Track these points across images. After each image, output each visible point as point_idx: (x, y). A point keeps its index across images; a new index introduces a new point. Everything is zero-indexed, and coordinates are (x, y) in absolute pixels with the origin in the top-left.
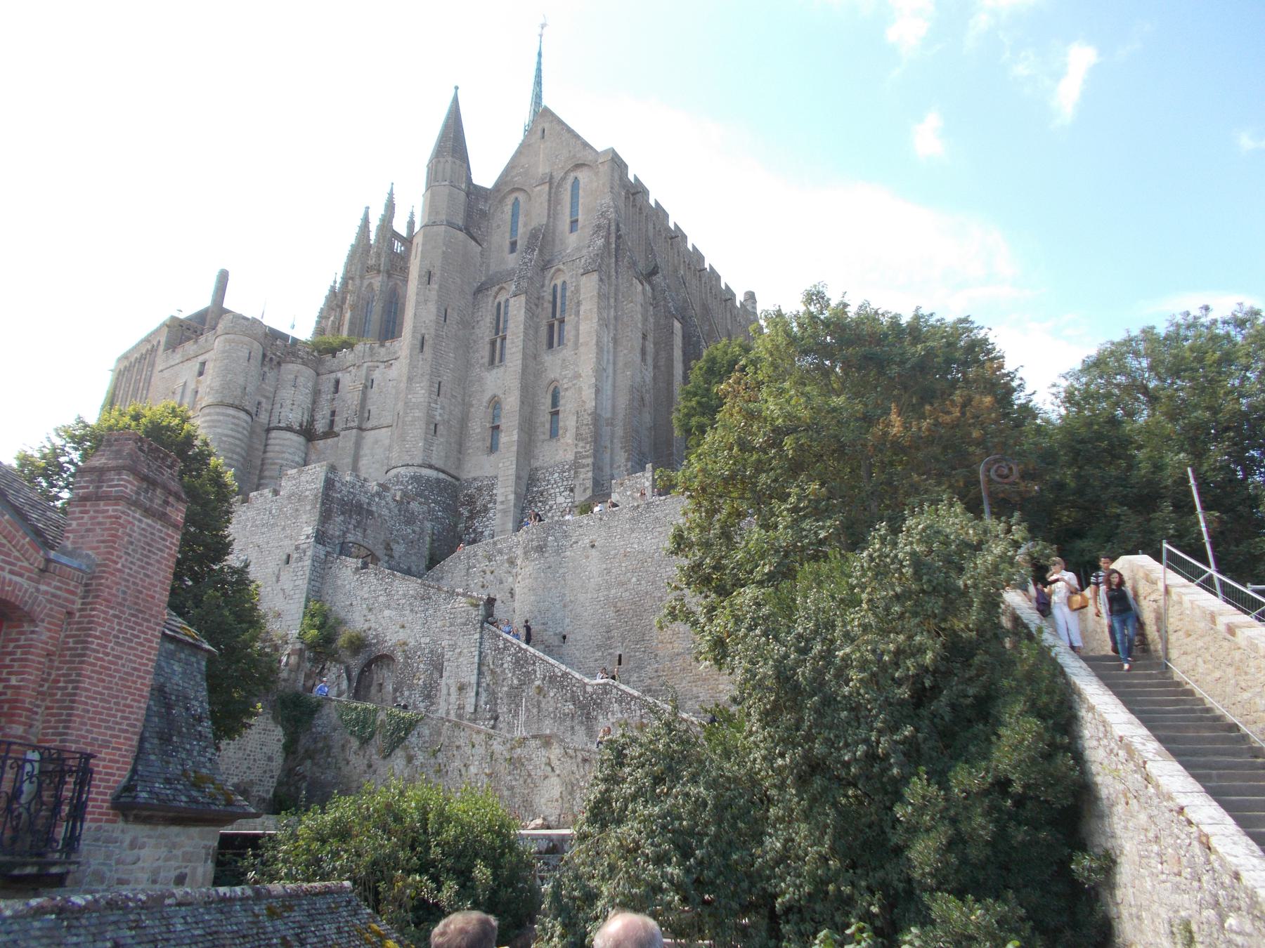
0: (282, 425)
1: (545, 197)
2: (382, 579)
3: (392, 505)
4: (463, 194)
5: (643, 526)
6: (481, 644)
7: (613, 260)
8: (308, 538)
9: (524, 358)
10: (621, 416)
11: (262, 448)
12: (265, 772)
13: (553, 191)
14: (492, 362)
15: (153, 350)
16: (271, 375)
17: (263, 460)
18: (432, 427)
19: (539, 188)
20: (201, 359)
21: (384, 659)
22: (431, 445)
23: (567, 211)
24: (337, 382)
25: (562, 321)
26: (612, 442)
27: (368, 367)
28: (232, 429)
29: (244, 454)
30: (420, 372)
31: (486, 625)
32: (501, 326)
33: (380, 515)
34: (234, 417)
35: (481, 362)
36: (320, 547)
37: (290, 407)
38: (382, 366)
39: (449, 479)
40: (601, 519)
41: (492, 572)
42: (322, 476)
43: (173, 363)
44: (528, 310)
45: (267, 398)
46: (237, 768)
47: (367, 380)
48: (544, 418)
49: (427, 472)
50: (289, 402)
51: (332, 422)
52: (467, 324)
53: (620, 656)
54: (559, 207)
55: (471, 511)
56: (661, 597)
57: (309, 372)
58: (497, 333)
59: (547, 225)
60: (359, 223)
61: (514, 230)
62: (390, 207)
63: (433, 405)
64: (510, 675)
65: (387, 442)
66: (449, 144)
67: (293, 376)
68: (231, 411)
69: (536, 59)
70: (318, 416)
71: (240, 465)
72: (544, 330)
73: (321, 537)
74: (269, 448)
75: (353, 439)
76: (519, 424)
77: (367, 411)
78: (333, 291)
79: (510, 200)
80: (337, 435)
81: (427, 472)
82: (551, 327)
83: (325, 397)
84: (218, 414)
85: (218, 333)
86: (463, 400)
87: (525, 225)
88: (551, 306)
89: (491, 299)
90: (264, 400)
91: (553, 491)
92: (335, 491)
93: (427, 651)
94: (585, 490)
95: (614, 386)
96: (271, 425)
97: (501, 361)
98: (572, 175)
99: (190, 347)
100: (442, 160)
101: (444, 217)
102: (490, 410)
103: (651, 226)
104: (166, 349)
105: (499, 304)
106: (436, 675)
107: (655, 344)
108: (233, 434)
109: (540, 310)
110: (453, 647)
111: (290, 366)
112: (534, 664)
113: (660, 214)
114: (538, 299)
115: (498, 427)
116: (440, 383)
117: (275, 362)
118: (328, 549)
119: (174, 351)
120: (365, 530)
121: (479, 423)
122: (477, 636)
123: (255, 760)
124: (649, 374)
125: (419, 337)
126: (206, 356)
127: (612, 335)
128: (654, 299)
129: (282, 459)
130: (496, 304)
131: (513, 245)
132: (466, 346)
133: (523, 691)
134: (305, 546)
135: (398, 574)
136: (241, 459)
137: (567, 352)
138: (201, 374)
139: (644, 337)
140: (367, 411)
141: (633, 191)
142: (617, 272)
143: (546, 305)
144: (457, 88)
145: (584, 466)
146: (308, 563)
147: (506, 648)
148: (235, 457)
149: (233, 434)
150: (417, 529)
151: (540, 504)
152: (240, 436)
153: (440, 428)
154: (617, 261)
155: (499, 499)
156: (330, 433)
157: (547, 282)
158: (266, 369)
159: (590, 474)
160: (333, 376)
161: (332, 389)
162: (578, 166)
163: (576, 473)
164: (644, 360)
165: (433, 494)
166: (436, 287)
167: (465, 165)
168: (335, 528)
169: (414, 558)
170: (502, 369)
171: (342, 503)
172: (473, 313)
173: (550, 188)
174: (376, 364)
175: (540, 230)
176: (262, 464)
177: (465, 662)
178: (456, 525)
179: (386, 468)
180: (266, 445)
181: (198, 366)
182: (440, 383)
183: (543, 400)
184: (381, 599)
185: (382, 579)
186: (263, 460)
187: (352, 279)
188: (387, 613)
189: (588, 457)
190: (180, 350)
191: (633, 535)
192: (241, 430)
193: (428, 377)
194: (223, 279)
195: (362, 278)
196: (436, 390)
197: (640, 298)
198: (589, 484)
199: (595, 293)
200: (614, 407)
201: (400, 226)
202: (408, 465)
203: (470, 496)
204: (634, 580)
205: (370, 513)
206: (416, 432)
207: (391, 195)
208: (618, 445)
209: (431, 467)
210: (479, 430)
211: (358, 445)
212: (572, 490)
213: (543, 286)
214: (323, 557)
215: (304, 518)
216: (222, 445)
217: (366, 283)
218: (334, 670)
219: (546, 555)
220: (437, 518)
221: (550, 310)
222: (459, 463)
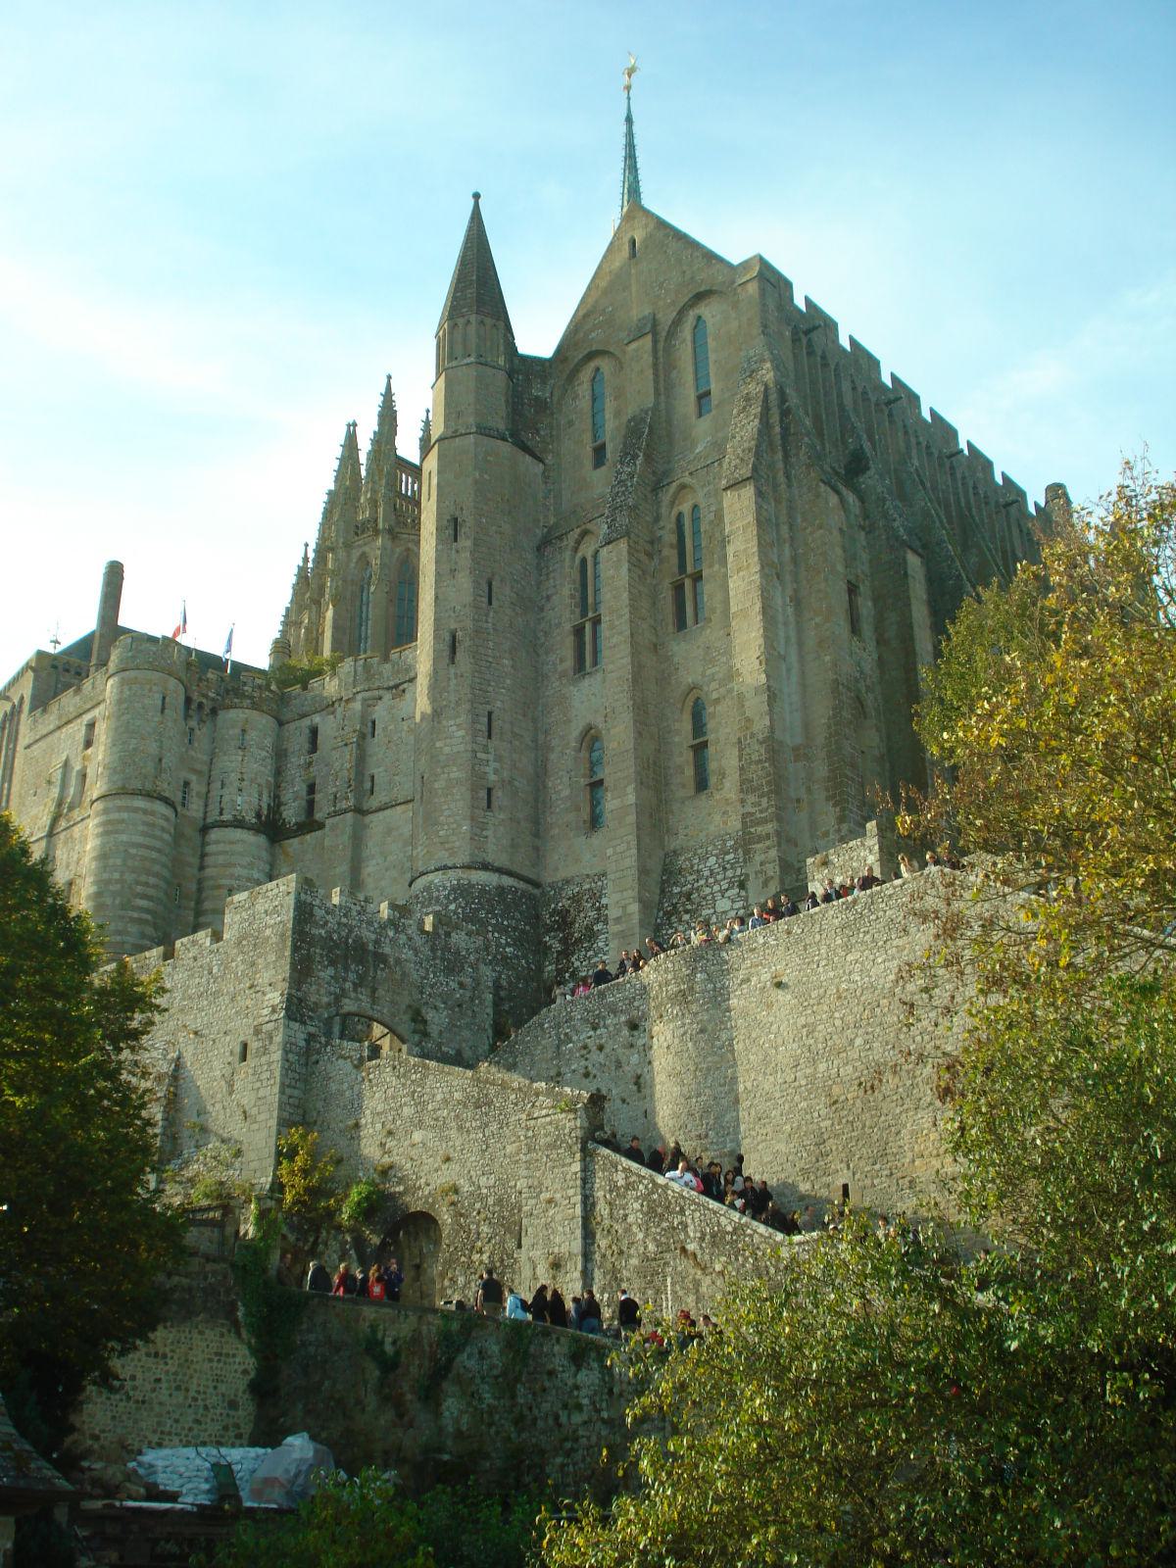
0: (226, 817)
1: (648, 358)
2: (404, 1075)
3: (419, 941)
4: (501, 376)
5: (868, 937)
6: (584, 1181)
7: (780, 455)
8: (274, 1011)
9: (635, 653)
10: (820, 738)
11: (195, 861)
12: (226, 1428)
13: (661, 345)
14: (579, 665)
15: (15, 712)
16: (202, 733)
17: (200, 882)
18: (483, 794)
19: (634, 346)
20: (87, 718)
21: (423, 1223)
22: (483, 827)
23: (689, 378)
24: (314, 732)
26: (809, 790)
28: (144, 834)
29: (166, 873)
30: (453, 698)
31: (591, 1145)
32: (590, 600)
33: (398, 961)
34: (145, 812)
35: (560, 668)
36: (296, 1026)
37: (237, 784)
38: (387, 696)
39: (522, 885)
40: (789, 933)
41: (601, 1048)
42: (291, 901)
43: (45, 732)
44: (635, 564)
45: (198, 772)
46: (177, 1421)
47: (363, 723)
48: (684, 759)
49: (480, 877)
50: (234, 777)
51: (311, 805)
52: (532, 604)
53: (845, 1187)
54: (674, 374)
55: (564, 941)
57: (262, 722)
58: (584, 613)
59: (655, 408)
60: (339, 451)
61: (596, 429)
62: (388, 416)
64: (641, 1236)
65: (406, 830)
66: (471, 292)
67: (237, 731)
68: (140, 803)
69: (624, 129)
70: (287, 796)
71: (161, 895)
72: (667, 595)
73: (296, 1008)
74: (209, 860)
75: (349, 830)
76: (638, 773)
77: (367, 779)
78: (302, 574)
79: (586, 375)
80: (321, 826)
81: (480, 877)
82: (679, 588)
83: (296, 761)
84: (120, 809)
85: (111, 671)
86: (535, 741)
87: (617, 414)
88: (675, 552)
89: (568, 554)
90: (193, 778)
91: (708, 890)
92: (317, 926)
93: (491, 1201)
94: (765, 884)
95: (803, 686)
96: (209, 820)
97: (595, 663)
98: (692, 314)
99: (69, 701)
100: (461, 321)
101: (471, 420)
102: (584, 754)
103: (846, 386)
104: (33, 709)
105: (584, 561)
106: (511, 1244)
107: (875, 600)
108: (148, 841)
109: (656, 560)
110: (536, 1189)
111: (233, 714)
112: (682, 1211)
113: (862, 361)
114: (652, 543)
115: (601, 782)
116: (490, 714)
117: (207, 710)
118: (312, 1030)
119: (45, 711)
120: (374, 990)
121: (566, 779)
122: (577, 1167)
123: (206, 1408)
124: (869, 660)
125: (448, 637)
126: (96, 712)
127: (789, 592)
128: (866, 517)
129: (232, 876)
130: (577, 561)
131: (599, 452)
132: (533, 645)
133: (666, 1264)
134: (271, 1026)
135: (432, 1064)
136: (162, 884)
137: (710, 634)
138: (88, 744)
139: (852, 589)
140: (367, 779)
141: (803, 327)
142: (788, 477)
143: (666, 552)
144: (477, 196)
145: (760, 839)
146: (277, 1055)
147: (629, 1186)
148: (152, 880)
149: (148, 841)
150: (468, 981)
151: (686, 917)
152: (158, 844)
153: (498, 794)
154: (786, 456)
155: (613, 913)
156: (310, 824)
157: (664, 511)
158: (193, 723)
159: (773, 853)
160: (306, 722)
161: (307, 746)
162: (700, 297)
163: (747, 852)
164: (855, 628)
165: (495, 916)
166: (468, 543)
167: (501, 324)
168: (319, 993)
169: (466, 1033)
170: (599, 676)
171: (330, 946)
172: (539, 584)
173: (655, 342)
174: (376, 693)
175: (643, 420)
176: (200, 890)
177: (558, 1217)
178: (540, 969)
179: (408, 876)
180: (203, 855)
181: (84, 728)
182: (490, 714)
183: (677, 725)
184: (407, 1111)
185: (404, 1075)
186: (200, 882)
187: (332, 549)
188: (417, 1136)
189: (765, 821)
190: (54, 707)
191: (850, 958)
192: (158, 833)
193: (467, 706)
194: (115, 575)
195: (348, 546)
196: (484, 728)
197: (837, 519)
198: (773, 870)
199: (751, 518)
200: (807, 726)
201: (407, 446)
202: (445, 868)
203: (564, 914)
204: (859, 1041)
205: (381, 958)
206: (455, 807)
207: (388, 396)
208: (820, 795)
209: (485, 867)
210: (566, 793)
211: (357, 840)
212: (742, 886)
213: (657, 519)
214: (302, 1043)
215: (264, 978)
216: (130, 863)
217: (356, 554)
218: (334, 1245)
220: (505, 958)
221: (675, 560)
222: (538, 854)
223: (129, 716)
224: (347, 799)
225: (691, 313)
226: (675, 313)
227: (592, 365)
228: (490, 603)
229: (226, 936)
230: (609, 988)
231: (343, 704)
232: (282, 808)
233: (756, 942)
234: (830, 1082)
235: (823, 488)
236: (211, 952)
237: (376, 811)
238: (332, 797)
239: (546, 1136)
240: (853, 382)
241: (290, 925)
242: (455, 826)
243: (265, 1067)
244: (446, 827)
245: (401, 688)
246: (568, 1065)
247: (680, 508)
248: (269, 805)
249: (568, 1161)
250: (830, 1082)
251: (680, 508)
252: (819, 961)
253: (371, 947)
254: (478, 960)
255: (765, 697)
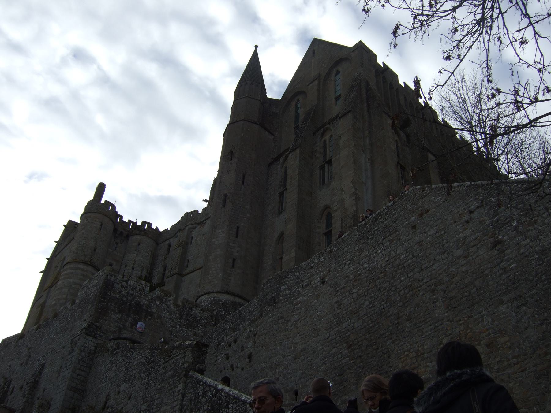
7: (365, 105)
19: (311, 85)
24: (169, 245)
25: (330, 162)
27: (189, 229)
34: (83, 270)
36: (91, 338)
51: (164, 275)
56: (398, 314)
63: (231, 244)
68: (81, 266)
79: (293, 104)
82: (322, 168)
116: (238, 228)
118: (100, 342)
122: (180, 387)
144: (256, 47)
160: (168, 242)
174: (194, 226)
182: (238, 228)
202: (209, 293)
204: (367, 303)
209: (228, 293)
214: (93, 348)
219: (279, 305)
223: (84, 231)
224: (175, 269)
225: (334, 70)
226: (327, 70)
227: (296, 99)
228: (243, 183)
229: (76, 301)
230: (243, 309)
231: (181, 231)
232: (153, 278)
233: (314, 262)
234: (349, 333)
235: (384, 115)
236: (70, 310)
237: (188, 274)
238: (170, 269)
239: (170, 371)
240: (405, 98)
241: (99, 290)
242: (216, 274)
243: (70, 360)
244: (212, 275)
245: (204, 222)
246: (221, 355)
247: (325, 138)
248: (146, 276)
249: (177, 384)
250: (349, 333)
251: (325, 138)
252: (346, 262)
253: (144, 307)
254: (206, 323)
255: (354, 198)
